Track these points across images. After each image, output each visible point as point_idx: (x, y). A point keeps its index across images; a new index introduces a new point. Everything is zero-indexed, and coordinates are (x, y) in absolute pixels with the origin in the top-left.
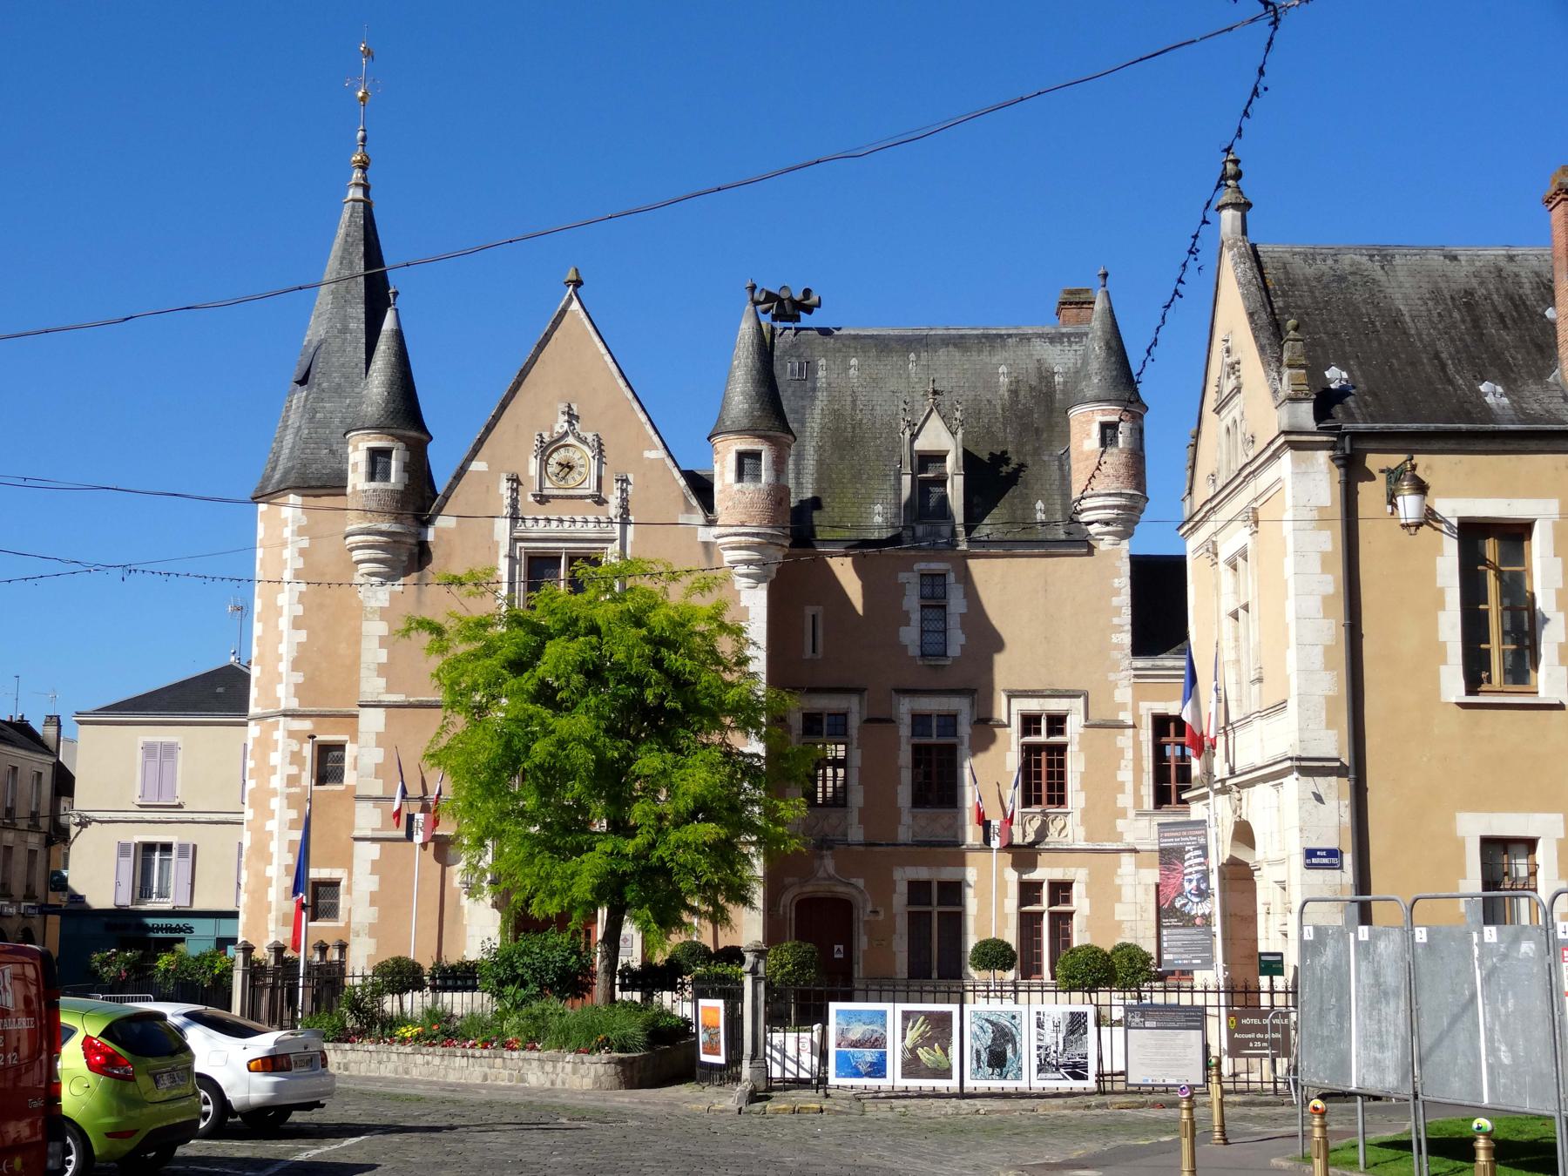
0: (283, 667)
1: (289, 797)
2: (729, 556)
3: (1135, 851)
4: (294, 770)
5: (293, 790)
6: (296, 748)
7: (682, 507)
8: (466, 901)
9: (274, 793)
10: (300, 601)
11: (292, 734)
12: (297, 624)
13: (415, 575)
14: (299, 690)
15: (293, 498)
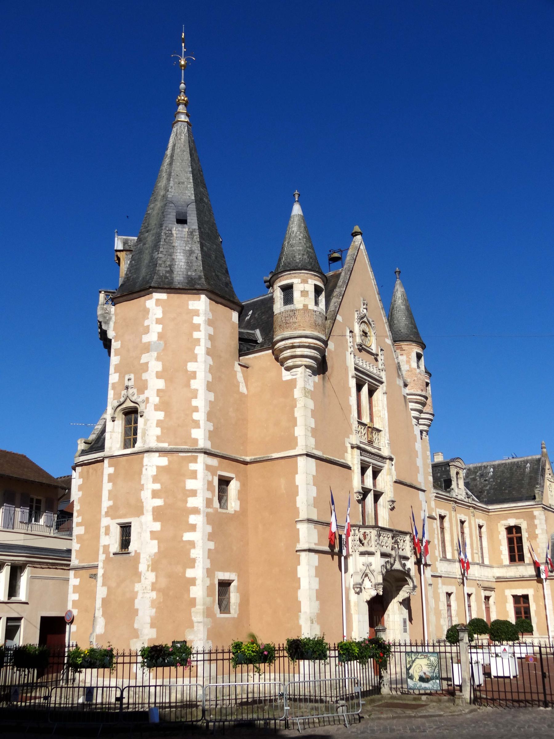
0: (200, 416)
1: (208, 515)
2: (412, 405)
3: (441, 577)
4: (209, 495)
5: (210, 510)
6: (210, 479)
7: (397, 375)
8: (353, 597)
9: (195, 511)
10: (210, 371)
11: (208, 468)
12: (210, 387)
13: (321, 375)
14: (212, 435)
15: (203, 297)
